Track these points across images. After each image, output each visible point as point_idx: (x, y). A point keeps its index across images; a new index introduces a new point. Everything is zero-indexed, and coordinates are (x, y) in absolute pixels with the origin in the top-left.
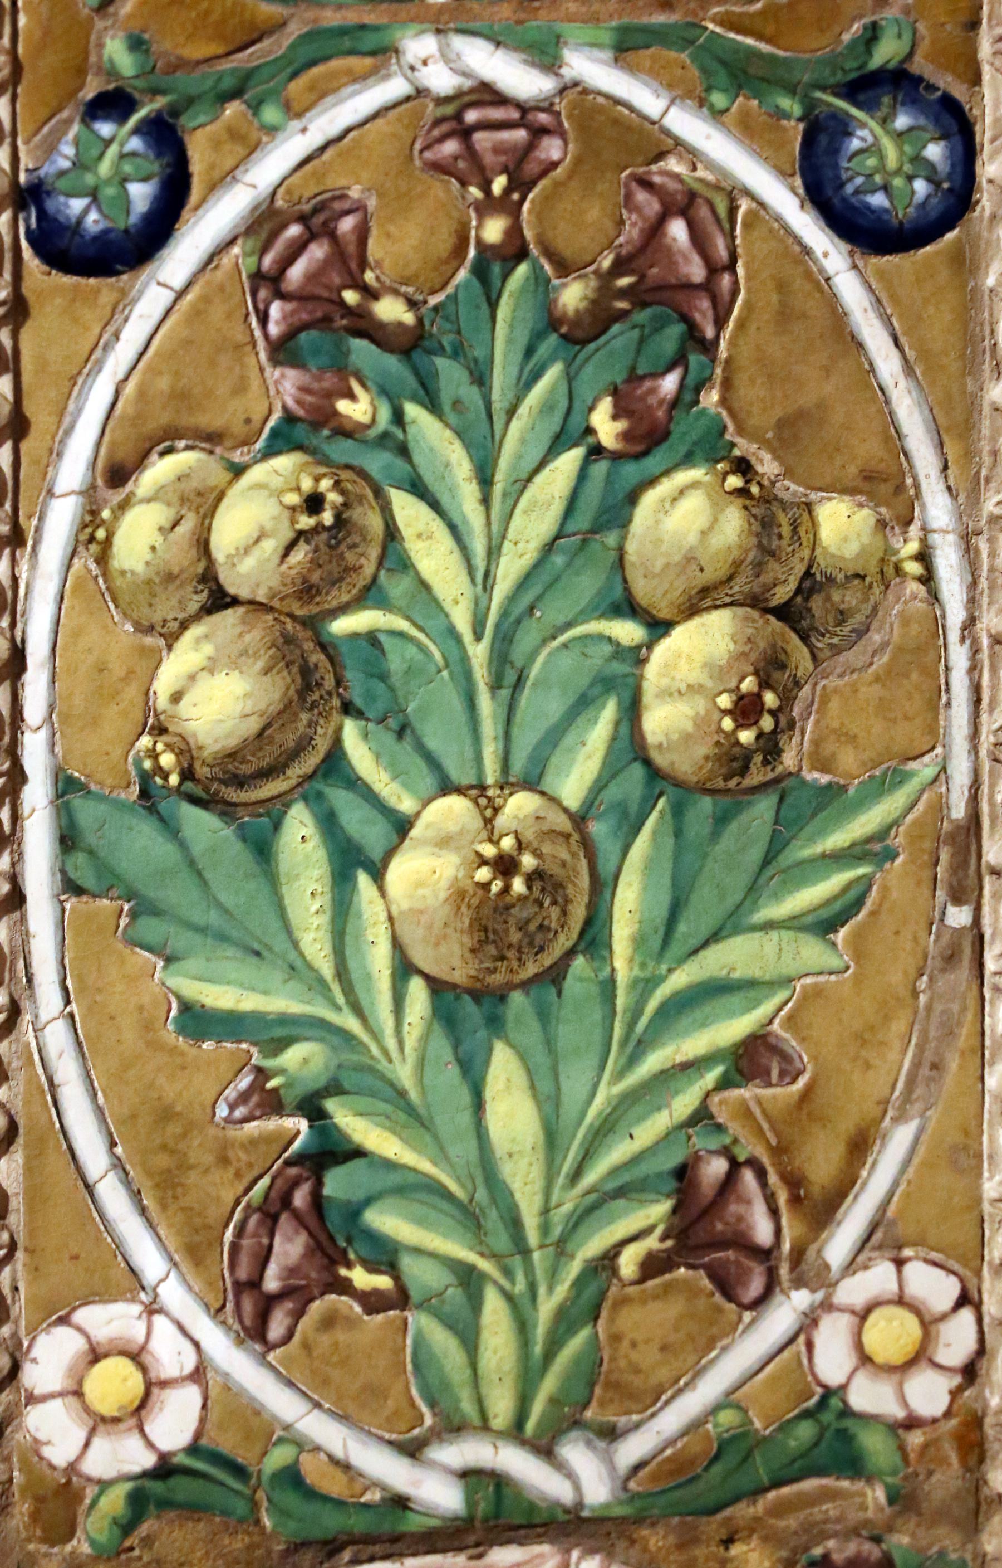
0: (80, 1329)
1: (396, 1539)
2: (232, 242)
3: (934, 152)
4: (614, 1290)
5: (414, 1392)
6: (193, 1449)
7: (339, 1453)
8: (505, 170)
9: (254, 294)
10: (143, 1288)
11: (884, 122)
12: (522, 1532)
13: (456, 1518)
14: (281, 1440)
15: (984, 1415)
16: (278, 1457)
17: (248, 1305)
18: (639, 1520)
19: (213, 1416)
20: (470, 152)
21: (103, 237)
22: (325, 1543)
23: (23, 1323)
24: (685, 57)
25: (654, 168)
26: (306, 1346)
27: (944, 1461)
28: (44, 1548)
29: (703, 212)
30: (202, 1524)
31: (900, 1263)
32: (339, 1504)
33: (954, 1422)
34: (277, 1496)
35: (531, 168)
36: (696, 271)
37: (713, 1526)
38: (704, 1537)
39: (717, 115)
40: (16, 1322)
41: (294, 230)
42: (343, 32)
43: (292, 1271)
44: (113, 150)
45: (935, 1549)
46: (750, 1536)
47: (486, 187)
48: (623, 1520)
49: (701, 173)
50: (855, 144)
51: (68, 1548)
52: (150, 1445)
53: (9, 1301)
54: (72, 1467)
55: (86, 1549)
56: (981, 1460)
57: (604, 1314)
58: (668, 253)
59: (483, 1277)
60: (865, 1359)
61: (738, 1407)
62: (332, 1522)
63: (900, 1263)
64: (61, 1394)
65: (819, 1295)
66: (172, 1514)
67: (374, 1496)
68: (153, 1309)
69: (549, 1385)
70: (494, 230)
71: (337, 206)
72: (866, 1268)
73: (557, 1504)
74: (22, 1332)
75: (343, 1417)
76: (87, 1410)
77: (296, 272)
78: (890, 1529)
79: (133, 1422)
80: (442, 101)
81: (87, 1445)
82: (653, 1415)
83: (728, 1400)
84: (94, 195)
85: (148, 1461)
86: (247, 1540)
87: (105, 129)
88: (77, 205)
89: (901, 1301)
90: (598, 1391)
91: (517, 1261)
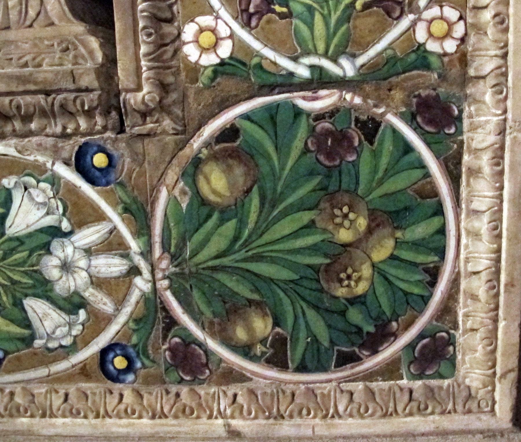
0: (197, 23)
1: (291, 85)
4: (354, 14)
5: (295, 43)
6: (231, 58)
7: (273, 59)
10: (214, 12)
12: (328, 85)
13: (308, 79)
14: (256, 56)
15: (467, 53)
16: (255, 61)
17: (245, 16)
18: (363, 81)
19: (236, 49)
22: (270, 86)
23: (181, 22)
26: (263, 29)
27: (455, 66)
28: (190, 85)
30: (234, 80)
31: (441, 7)
32: (274, 74)
33: (458, 55)
34: (255, 71)
37: (385, 84)
38: (383, 87)
40: (179, 22)
43: (257, 6)
45: (452, 93)
46: (396, 88)
48: (358, 81)
51: (197, 85)
52: (218, 56)
53: (177, 16)
54: (197, 63)
55: (201, 85)
56: (466, 65)
57: (352, 21)
59: (315, 9)
60: (430, 35)
61: (393, 49)
62: (272, 80)
63: (441, 7)
64: (192, 42)
65: (417, 16)
66: (225, 76)
67: (284, 72)
68: (217, 18)
69: (335, 41)
72: (431, 8)
73: (339, 76)
74: (181, 25)
75: (274, 49)
76: (200, 46)
78: (439, 86)
79: (213, 50)
81: (200, 56)
82: (367, 51)
83: (390, 46)
85: (218, 61)
86: (247, 85)
89: (442, 18)
90: (350, 43)
91: (325, 4)
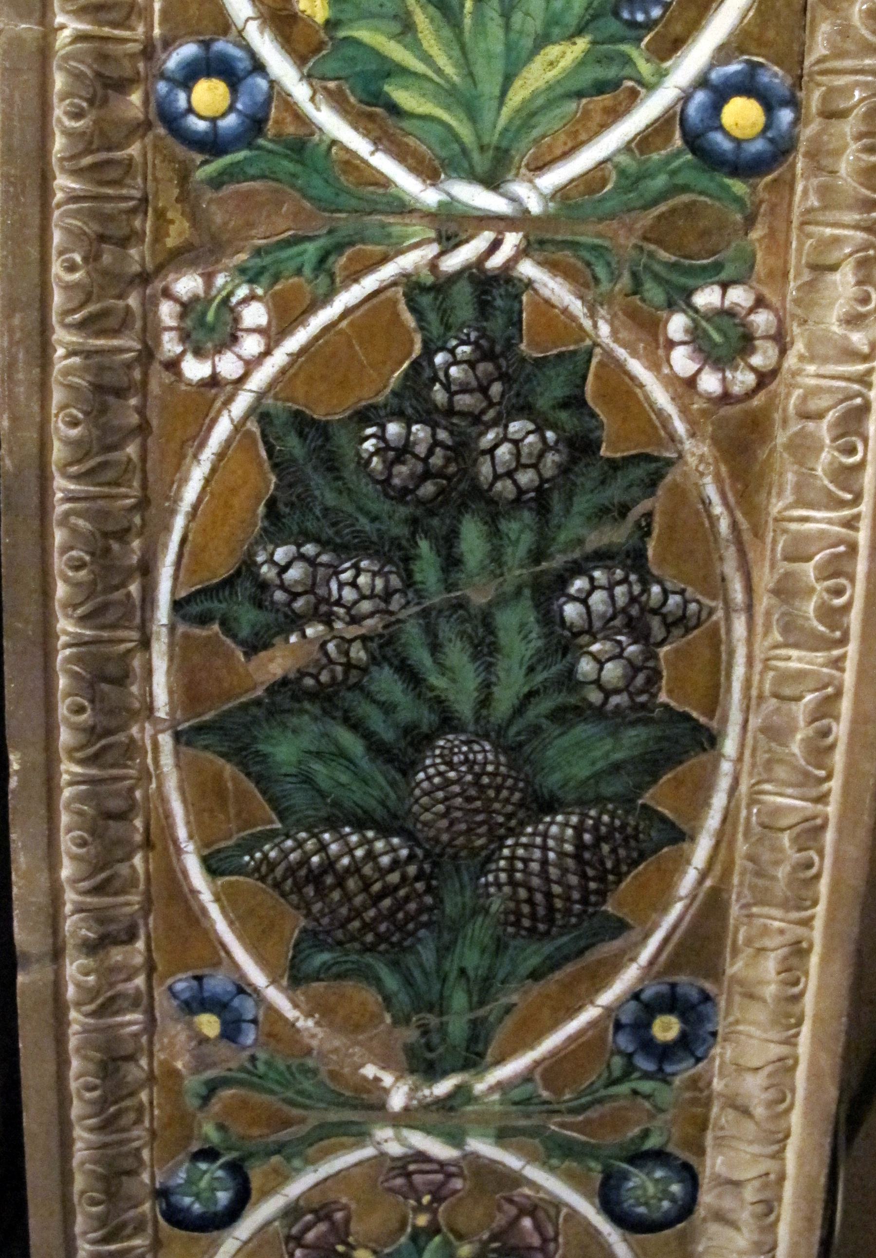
2: (274, 1220)
3: (675, 1188)
8: (430, 1192)
9: (287, 1244)
11: (648, 1174)
20: (411, 1185)
21: (202, 1216)
24: (537, 1141)
25: (515, 1192)
29: (541, 1214)
35: (444, 1192)
36: (536, 1241)
39: (552, 1170)
41: (309, 1217)
42: (340, 1124)
44: (207, 1177)
47: (419, 1200)
49: (541, 1195)
50: (631, 1184)
58: (522, 1232)
70: (422, 1220)
71: (333, 1206)
77: (310, 1236)
80: (394, 1159)
84: (197, 1196)
87: (203, 1166)
88: (187, 1200)
